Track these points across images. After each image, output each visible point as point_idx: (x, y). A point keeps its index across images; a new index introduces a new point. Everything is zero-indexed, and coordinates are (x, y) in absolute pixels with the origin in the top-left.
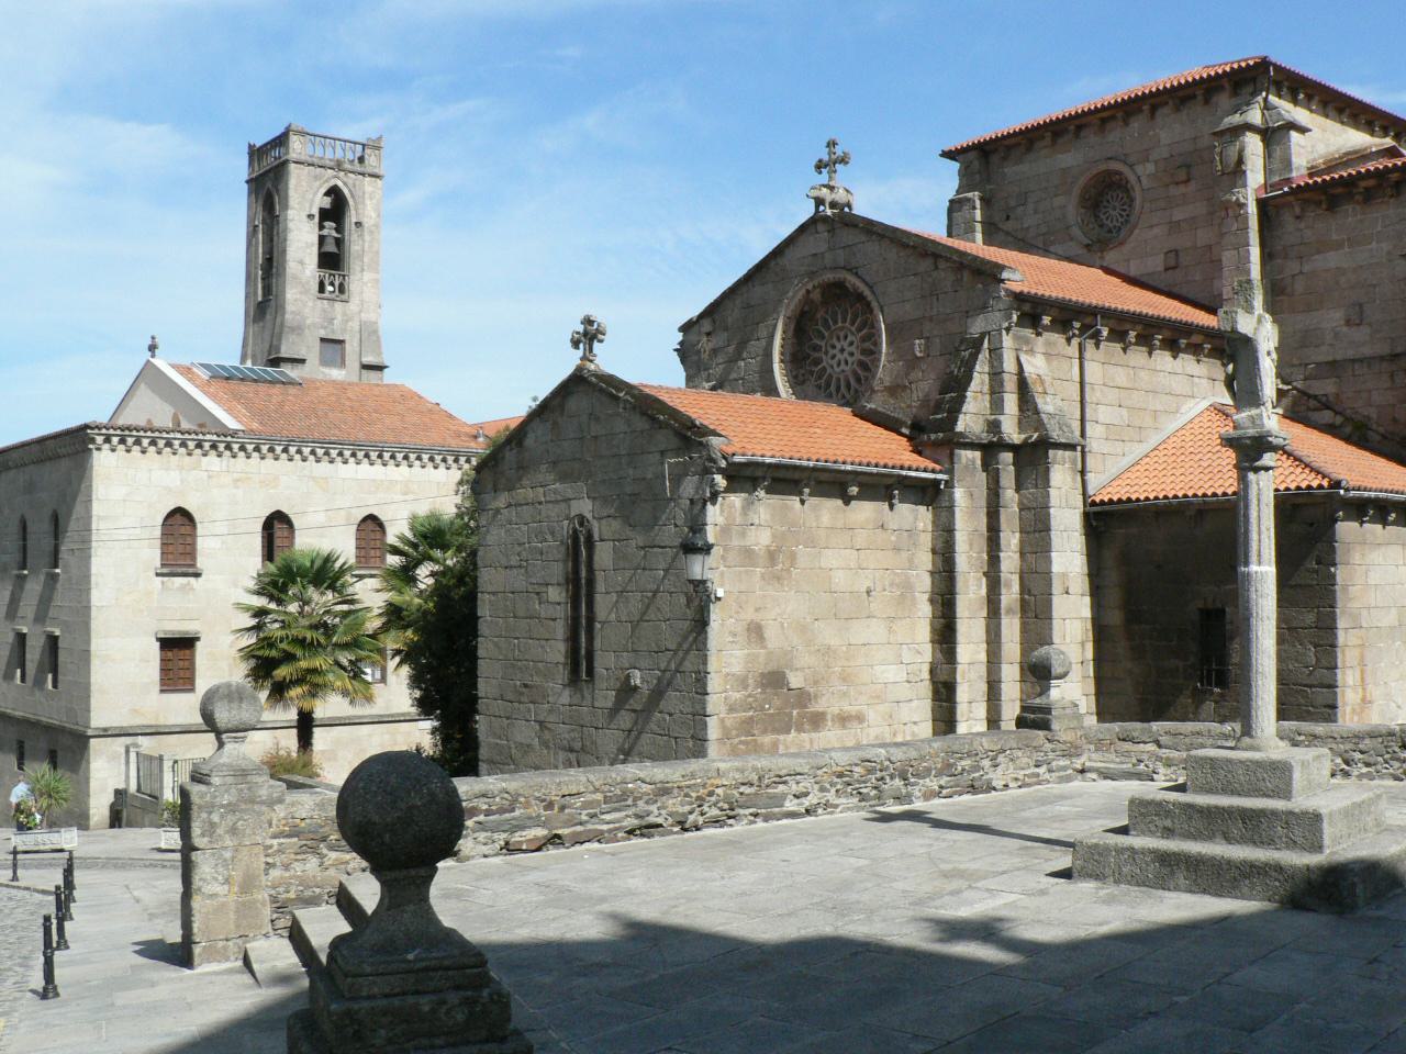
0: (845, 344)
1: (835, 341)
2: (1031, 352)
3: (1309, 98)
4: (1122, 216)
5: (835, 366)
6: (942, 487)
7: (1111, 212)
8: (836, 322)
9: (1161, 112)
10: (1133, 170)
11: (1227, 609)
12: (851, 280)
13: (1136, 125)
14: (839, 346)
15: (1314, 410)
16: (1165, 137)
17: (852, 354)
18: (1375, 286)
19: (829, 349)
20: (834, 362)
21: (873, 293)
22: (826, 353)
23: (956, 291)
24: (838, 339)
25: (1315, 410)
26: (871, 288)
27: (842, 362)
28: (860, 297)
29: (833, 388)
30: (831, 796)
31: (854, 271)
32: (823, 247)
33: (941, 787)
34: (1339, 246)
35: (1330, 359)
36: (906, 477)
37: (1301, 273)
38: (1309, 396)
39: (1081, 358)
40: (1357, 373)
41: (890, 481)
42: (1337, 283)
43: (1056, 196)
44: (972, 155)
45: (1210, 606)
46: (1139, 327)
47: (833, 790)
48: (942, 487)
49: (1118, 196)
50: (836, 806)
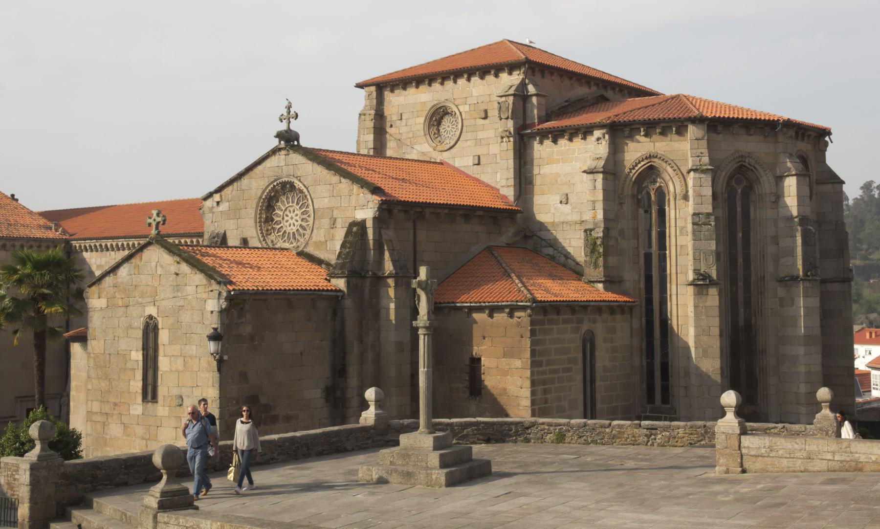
0: (293, 215)
1: (288, 214)
2: (388, 228)
3: (552, 74)
4: (452, 131)
5: (288, 226)
6: (340, 298)
7: (447, 128)
8: (288, 203)
9: (473, 79)
10: (458, 108)
12: (298, 184)
13: (460, 83)
14: (290, 216)
15: (544, 247)
17: (297, 221)
18: (574, 184)
19: (285, 217)
20: (287, 224)
21: (308, 192)
22: (283, 219)
24: (290, 211)
25: (546, 247)
26: (307, 189)
27: (292, 225)
28: (301, 191)
29: (289, 238)
30: (275, 455)
31: (299, 178)
32: (282, 163)
33: (323, 450)
34: (557, 162)
36: (321, 295)
38: (542, 239)
39: (415, 229)
41: (313, 297)
42: (557, 181)
43: (418, 117)
44: (373, 88)
46: (446, 211)
47: (276, 453)
48: (340, 298)
49: (450, 120)
50: (278, 459)
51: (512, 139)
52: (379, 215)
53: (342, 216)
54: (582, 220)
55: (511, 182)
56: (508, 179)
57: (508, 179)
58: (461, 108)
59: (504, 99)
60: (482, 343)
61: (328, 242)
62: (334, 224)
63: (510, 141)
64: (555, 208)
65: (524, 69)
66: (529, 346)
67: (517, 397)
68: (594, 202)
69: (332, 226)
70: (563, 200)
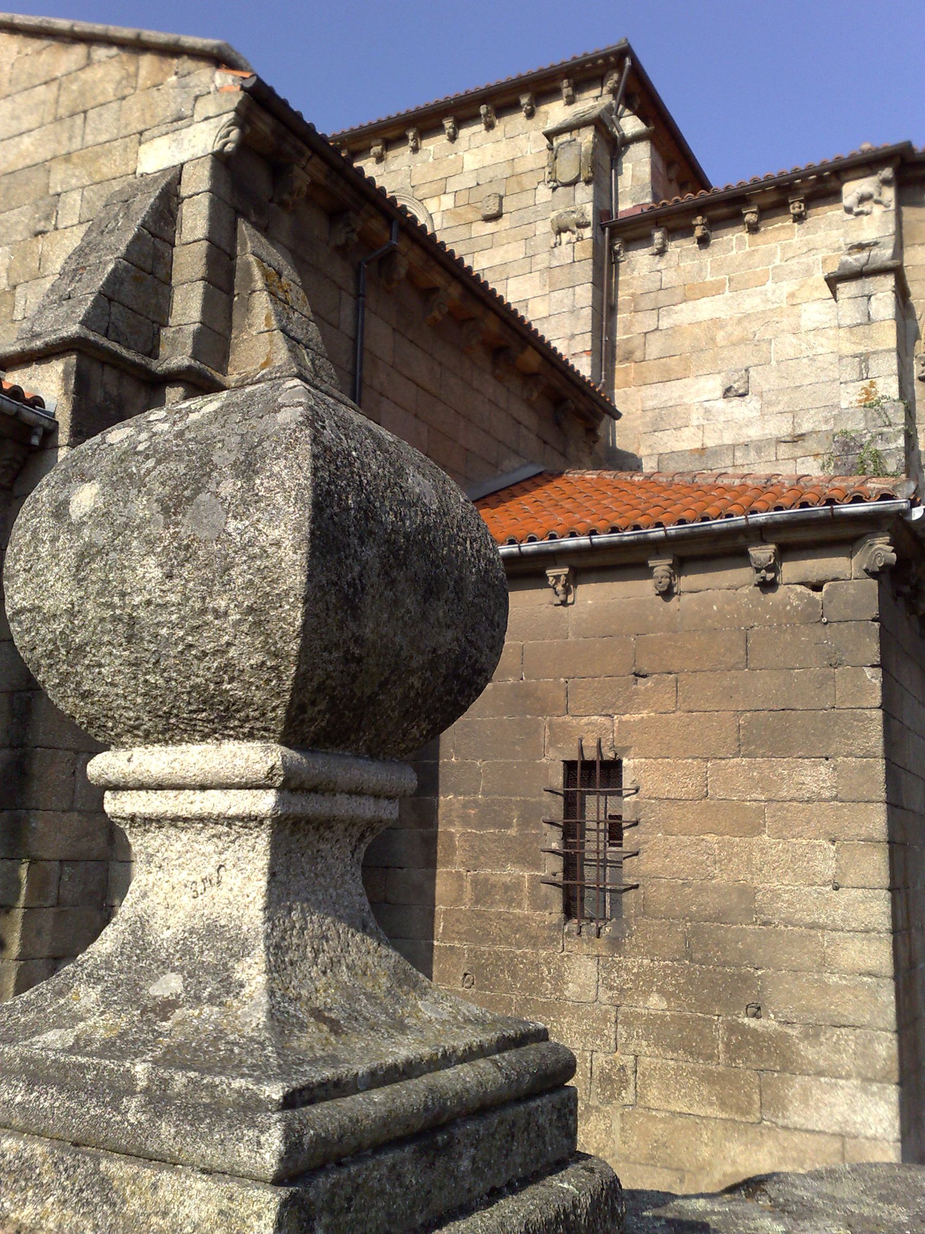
6: (35, 441)
11: (625, 762)
13: (431, 148)
16: (471, 161)
23: (124, 98)
34: (716, 289)
35: (698, 445)
37: (657, 329)
40: (738, 462)
42: (713, 339)
45: (590, 755)
48: (35, 441)
51: (588, 233)
52: (243, 144)
53: (86, 181)
54: (799, 431)
55: (585, 342)
56: (573, 336)
57: (573, 336)
58: (432, 205)
59: (566, 137)
60: (630, 699)
61: (19, 289)
62: (47, 218)
63: (580, 239)
64: (707, 411)
65: (615, 76)
66: (878, 702)
67: (813, 926)
68: (864, 359)
69: (40, 227)
70: (736, 386)
